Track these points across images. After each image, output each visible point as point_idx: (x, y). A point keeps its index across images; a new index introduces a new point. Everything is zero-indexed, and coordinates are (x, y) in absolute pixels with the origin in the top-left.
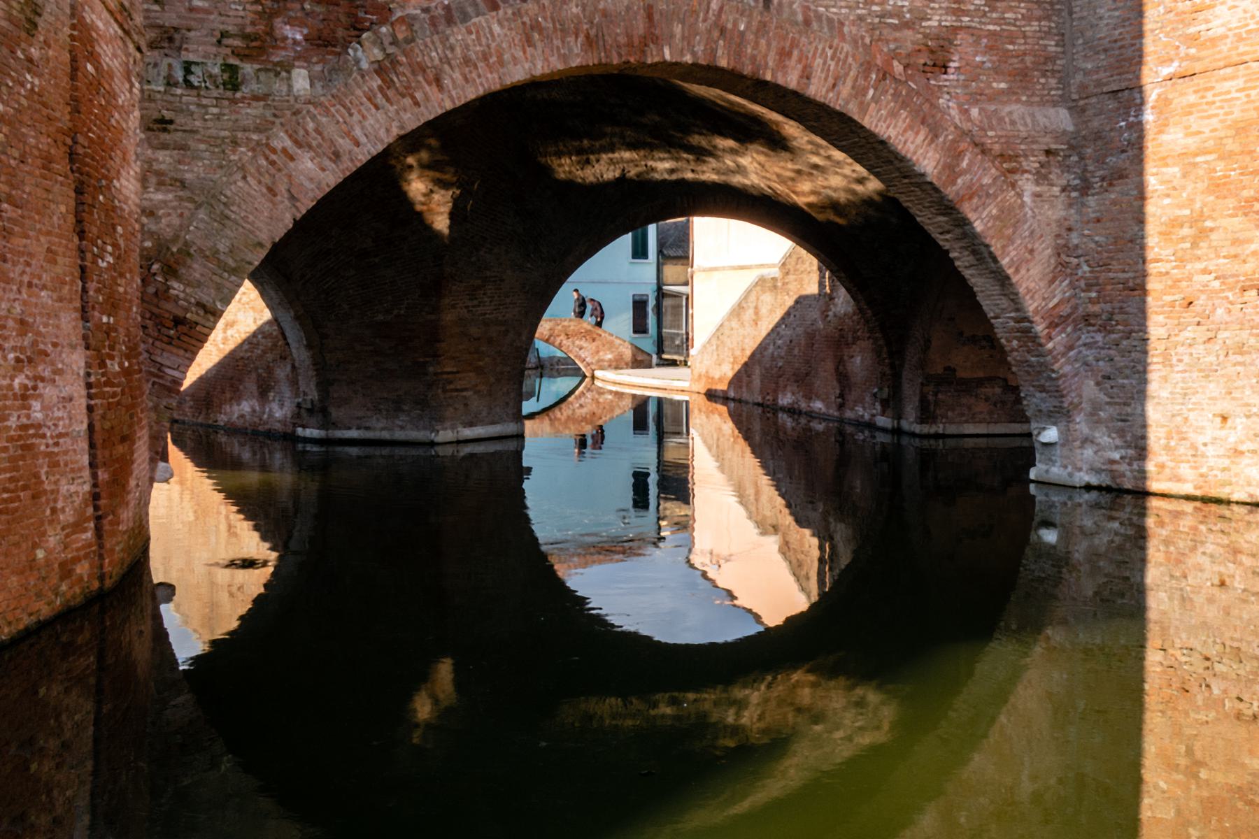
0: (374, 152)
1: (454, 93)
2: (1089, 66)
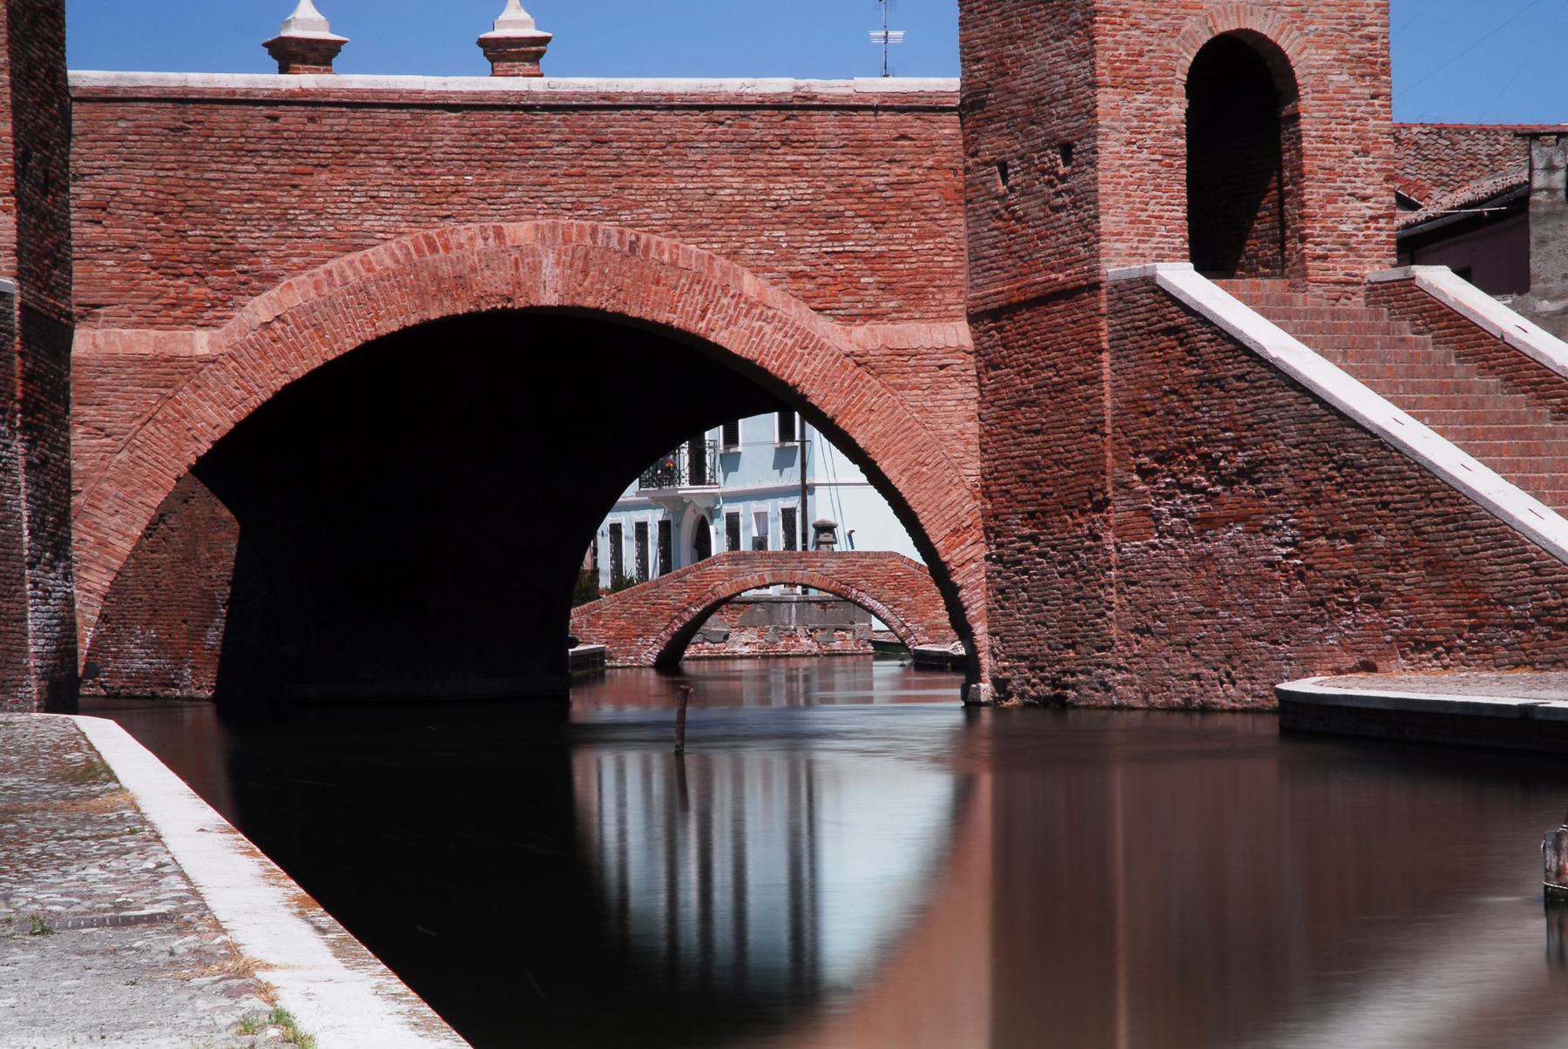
0: (265, 399)
1: (335, 347)
2: (979, 281)
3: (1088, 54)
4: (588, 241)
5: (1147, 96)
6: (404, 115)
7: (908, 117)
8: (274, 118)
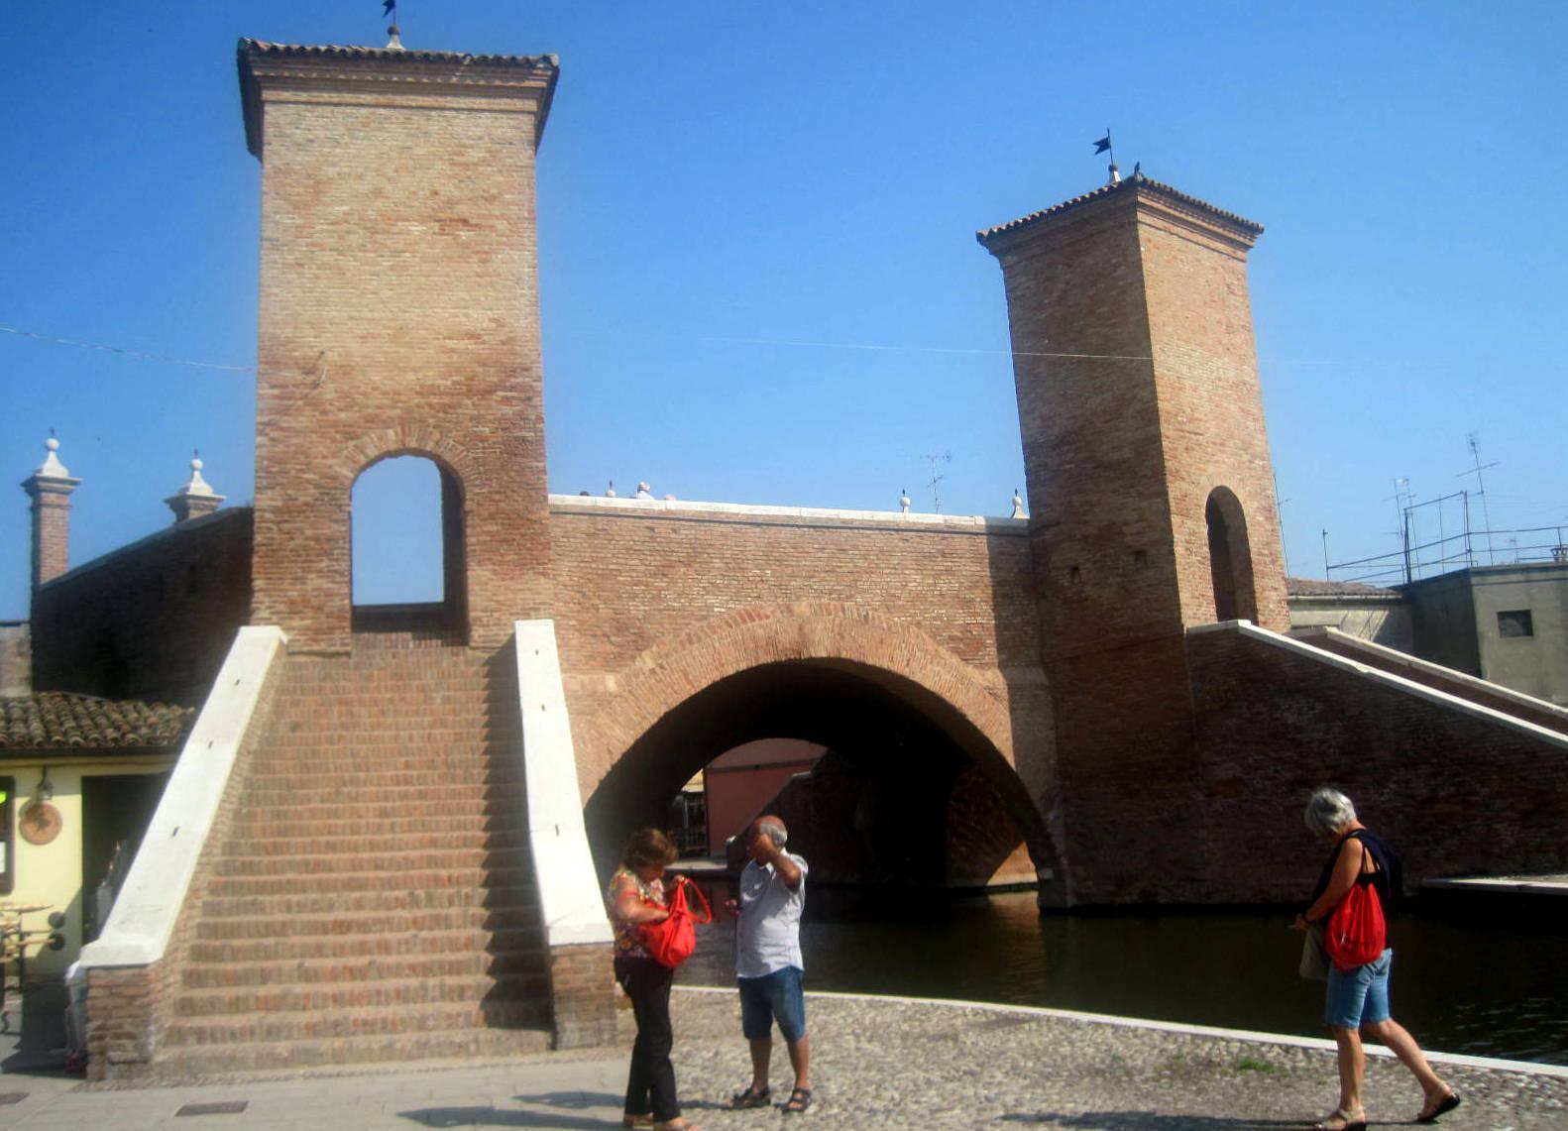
4: (841, 614)
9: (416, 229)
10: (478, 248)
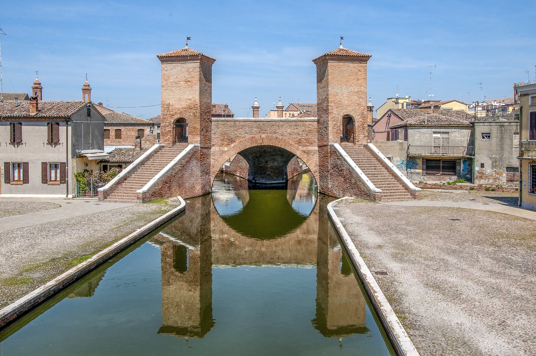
3: (328, 117)
5: (335, 122)
6: (250, 122)
7: (311, 122)
8: (235, 123)
9: (182, 83)
10: (191, 86)
